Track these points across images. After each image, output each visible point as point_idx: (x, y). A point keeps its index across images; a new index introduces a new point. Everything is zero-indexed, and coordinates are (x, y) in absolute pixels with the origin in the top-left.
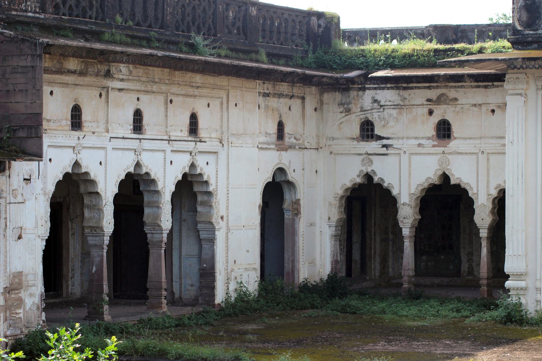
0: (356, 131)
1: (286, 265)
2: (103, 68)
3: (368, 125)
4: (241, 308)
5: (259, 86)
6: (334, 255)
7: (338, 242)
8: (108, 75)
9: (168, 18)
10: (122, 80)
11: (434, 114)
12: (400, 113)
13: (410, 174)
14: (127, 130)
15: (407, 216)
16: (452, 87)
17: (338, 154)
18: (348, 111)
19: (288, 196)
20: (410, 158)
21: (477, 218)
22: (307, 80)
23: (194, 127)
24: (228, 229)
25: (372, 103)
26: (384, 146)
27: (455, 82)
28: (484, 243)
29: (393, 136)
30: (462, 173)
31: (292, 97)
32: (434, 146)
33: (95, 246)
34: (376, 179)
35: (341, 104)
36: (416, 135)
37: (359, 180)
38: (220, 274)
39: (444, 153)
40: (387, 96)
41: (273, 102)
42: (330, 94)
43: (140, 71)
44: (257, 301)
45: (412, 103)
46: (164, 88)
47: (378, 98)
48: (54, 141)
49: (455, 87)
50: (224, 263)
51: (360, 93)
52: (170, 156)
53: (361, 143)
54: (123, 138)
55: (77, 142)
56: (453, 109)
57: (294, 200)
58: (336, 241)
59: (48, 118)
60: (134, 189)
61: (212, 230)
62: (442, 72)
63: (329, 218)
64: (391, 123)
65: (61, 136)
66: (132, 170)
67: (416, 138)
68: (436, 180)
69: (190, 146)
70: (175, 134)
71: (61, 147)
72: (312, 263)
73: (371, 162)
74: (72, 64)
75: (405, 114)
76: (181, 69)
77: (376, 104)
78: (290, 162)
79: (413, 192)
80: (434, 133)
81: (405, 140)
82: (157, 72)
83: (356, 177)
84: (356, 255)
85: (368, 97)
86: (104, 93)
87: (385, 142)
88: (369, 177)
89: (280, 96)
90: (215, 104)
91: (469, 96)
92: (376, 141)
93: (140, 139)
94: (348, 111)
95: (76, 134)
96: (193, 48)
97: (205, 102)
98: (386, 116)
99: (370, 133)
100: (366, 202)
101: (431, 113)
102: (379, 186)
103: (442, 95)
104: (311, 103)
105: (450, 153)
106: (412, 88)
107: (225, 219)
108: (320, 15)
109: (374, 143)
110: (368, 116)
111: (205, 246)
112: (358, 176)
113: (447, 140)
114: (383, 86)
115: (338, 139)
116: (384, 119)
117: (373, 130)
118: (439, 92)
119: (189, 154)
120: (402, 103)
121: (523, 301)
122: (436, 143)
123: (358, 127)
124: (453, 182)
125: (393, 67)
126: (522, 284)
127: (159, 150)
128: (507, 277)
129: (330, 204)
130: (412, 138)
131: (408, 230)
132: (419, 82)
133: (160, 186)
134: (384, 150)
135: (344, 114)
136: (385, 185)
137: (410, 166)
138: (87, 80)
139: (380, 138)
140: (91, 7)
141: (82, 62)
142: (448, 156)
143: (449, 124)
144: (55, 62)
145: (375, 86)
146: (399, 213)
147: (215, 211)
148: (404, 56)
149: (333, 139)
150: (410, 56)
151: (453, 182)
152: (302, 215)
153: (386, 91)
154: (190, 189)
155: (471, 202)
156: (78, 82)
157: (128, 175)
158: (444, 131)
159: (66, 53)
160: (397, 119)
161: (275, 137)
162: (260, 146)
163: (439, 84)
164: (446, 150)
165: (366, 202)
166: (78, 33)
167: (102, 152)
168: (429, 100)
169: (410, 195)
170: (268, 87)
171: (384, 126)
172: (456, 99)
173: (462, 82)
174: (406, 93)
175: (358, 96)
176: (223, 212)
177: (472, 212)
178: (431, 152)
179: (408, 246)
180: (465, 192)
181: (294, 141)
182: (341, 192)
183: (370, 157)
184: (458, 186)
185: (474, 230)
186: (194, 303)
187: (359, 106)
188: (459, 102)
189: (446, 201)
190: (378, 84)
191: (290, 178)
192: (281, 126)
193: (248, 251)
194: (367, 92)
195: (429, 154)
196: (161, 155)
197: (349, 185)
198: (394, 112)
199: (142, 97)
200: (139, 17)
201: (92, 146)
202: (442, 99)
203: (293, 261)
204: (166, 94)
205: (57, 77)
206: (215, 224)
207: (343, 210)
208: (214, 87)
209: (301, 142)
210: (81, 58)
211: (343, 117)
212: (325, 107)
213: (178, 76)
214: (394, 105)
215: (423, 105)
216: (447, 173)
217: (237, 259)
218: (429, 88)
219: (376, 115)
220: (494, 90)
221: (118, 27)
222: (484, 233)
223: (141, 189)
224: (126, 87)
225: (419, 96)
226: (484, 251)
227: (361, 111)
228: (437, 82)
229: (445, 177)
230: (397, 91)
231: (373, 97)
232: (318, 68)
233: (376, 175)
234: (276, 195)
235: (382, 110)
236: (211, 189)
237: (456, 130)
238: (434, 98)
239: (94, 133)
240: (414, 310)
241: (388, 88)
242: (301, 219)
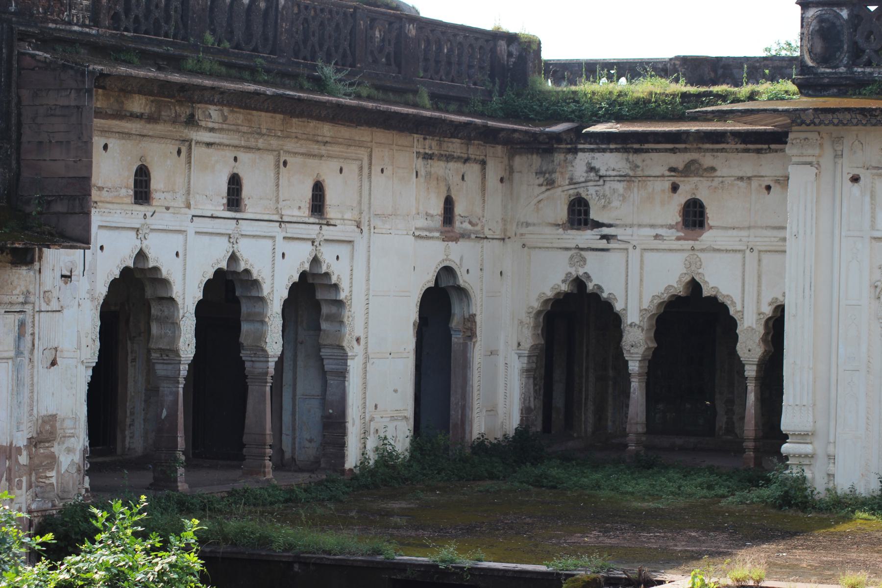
0: (562, 213)
1: (452, 412)
2: (184, 111)
3: (580, 205)
4: (384, 474)
5: (418, 143)
6: (525, 399)
7: (531, 380)
8: (191, 121)
9: (283, 38)
10: (212, 130)
11: (679, 191)
12: (628, 189)
13: (641, 280)
14: (217, 205)
15: (636, 343)
16: (707, 150)
17: (535, 248)
18: (551, 184)
19: (457, 310)
20: (642, 256)
21: (742, 349)
22: (489, 136)
23: (318, 204)
24: (367, 357)
25: (587, 172)
26: (603, 237)
27: (713, 143)
28: (751, 387)
29: (618, 222)
30: (721, 280)
31: (466, 161)
32: (679, 239)
33: (167, 378)
34: (590, 286)
35: (540, 173)
36: (653, 222)
37: (564, 288)
38: (353, 425)
39: (693, 249)
40: (610, 162)
41: (439, 167)
42: (525, 158)
43: (238, 117)
44: (408, 465)
45: (647, 174)
46: (274, 143)
47: (596, 164)
48: (108, 219)
49: (712, 150)
50: (360, 408)
51: (570, 157)
52: (282, 246)
53: (569, 231)
54: (212, 217)
55: (143, 221)
56: (709, 183)
57: (467, 316)
58: (528, 378)
59: (100, 185)
60: (228, 292)
61: (343, 358)
62: (693, 127)
63: (519, 344)
64: (616, 203)
65: (118, 212)
66: (224, 265)
67: (652, 226)
68: (679, 289)
69: (313, 231)
70: (289, 213)
71: (117, 228)
72: (492, 411)
73: (584, 260)
74: (138, 104)
75: (636, 190)
76: (300, 115)
77: (592, 174)
78: (461, 259)
79: (645, 306)
80: (680, 219)
81: (635, 229)
82: (264, 119)
83: (560, 283)
84: (559, 400)
85: (580, 163)
86: (185, 148)
87: (605, 231)
88: (579, 283)
89: (449, 158)
90: (351, 168)
91: (733, 165)
92: (592, 229)
93: (237, 219)
94: (551, 184)
95: (142, 209)
96: (320, 84)
97: (335, 165)
98: (607, 193)
99: (582, 217)
100: (575, 322)
101: (675, 188)
102: (596, 297)
103: (693, 162)
104: (494, 171)
105: (702, 250)
106: (647, 151)
107: (362, 342)
108: (511, 38)
109: (589, 232)
110: (581, 191)
111: (332, 381)
112: (564, 281)
113: (698, 230)
114: (604, 146)
115: (534, 225)
116: (604, 196)
117: (587, 213)
118: (688, 157)
119: (310, 243)
120: (631, 173)
122: (681, 234)
123: (566, 208)
124: (706, 293)
125: (619, 118)
127: (265, 237)
129: (521, 322)
130: (645, 226)
131: (637, 364)
132: (659, 143)
133: (266, 290)
134: (603, 244)
135: (544, 188)
136: (605, 295)
137: (642, 268)
138: (160, 128)
139: (598, 225)
140: (168, 20)
141: (152, 101)
142: (700, 255)
143: (702, 206)
144: (112, 100)
145: (592, 146)
146: (624, 339)
147: (347, 330)
148: (637, 102)
149: (528, 225)
150: (646, 102)
151: (706, 293)
152: (479, 338)
153: (608, 155)
154: (312, 296)
155: (731, 324)
156: (145, 132)
157: (219, 273)
158: (694, 216)
159: (129, 87)
160: (623, 196)
161: (439, 220)
162: (417, 233)
163: (688, 146)
164: (697, 245)
165: (575, 322)
166: (147, 58)
167: (180, 237)
168: (672, 169)
169: (641, 311)
170: (431, 145)
171: (604, 207)
172: (713, 169)
173: (723, 143)
174: (637, 159)
175: (565, 160)
176: (359, 331)
178: (674, 247)
179: (637, 387)
180: (724, 308)
181: (469, 227)
182: (536, 305)
183: (583, 253)
184: (713, 300)
186: (313, 467)
187: (567, 176)
188: (718, 173)
189: (694, 320)
190: (597, 144)
191: (461, 283)
192: (449, 204)
193: (396, 391)
194: (580, 155)
195: (671, 250)
196: (268, 243)
197: (550, 294)
198: (620, 187)
199: (243, 156)
200: (239, 35)
201: (165, 228)
202: (692, 168)
203: (464, 408)
204: (278, 152)
205: (115, 124)
206: (348, 350)
207: (540, 332)
208: (350, 143)
209: (478, 228)
210: (151, 95)
211: (543, 192)
212: (516, 176)
213: (296, 125)
214: (620, 176)
215: (663, 176)
216: (697, 279)
217: (379, 402)
218: (673, 151)
219: (592, 190)
220: (770, 156)
221: (207, 50)
222: (751, 371)
223: (237, 294)
224: (217, 141)
225: (657, 163)
226: (751, 398)
227: (570, 184)
228: (685, 143)
229: (694, 286)
230: (625, 155)
231: (589, 164)
232: (506, 118)
233: (591, 281)
234: (440, 308)
235: (601, 182)
236: (342, 296)
237: (712, 216)
238: (681, 166)
239: (168, 208)
240: (643, 485)
241: (611, 151)
242: (477, 345)
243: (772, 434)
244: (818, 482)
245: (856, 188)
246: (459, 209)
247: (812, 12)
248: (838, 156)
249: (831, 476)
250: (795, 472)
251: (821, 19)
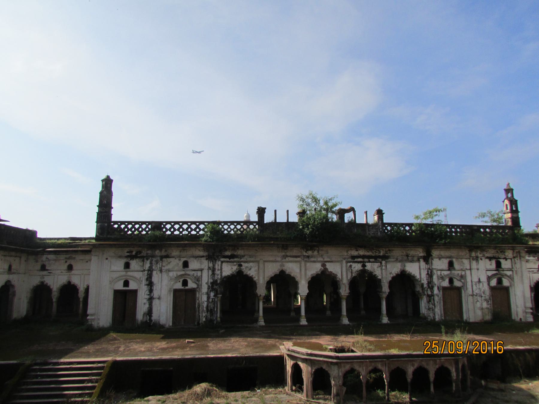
0: (39, 267)
15: (55, 295)
18: (37, 261)
22: (22, 251)
30: (76, 280)
31: (16, 257)
34: (45, 283)
37: (39, 284)
40: (51, 257)
41: (8, 258)
73: (44, 278)
88: (42, 283)
89: (11, 256)
101: (66, 262)
104: (23, 259)
118: (69, 255)
121: (93, 323)
126: (93, 317)
128: (88, 315)
139: (48, 270)
151: (72, 284)
165: (41, 292)
172: (74, 258)
174: (58, 256)
177: (78, 293)
179: (55, 305)
182: (32, 287)
185: (78, 299)
189: (69, 290)
197: (35, 285)
198: (54, 262)
222: (81, 300)
225: (62, 257)
226: (81, 305)
237: (74, 268)
243: (85, 314)
244: (95, 324)
245: (107, 261)
246: (13, 267)
247: (99, 224)
248: (103, 254)
249: (98, 323)
250: (90, 323)
251: (101, 226)
